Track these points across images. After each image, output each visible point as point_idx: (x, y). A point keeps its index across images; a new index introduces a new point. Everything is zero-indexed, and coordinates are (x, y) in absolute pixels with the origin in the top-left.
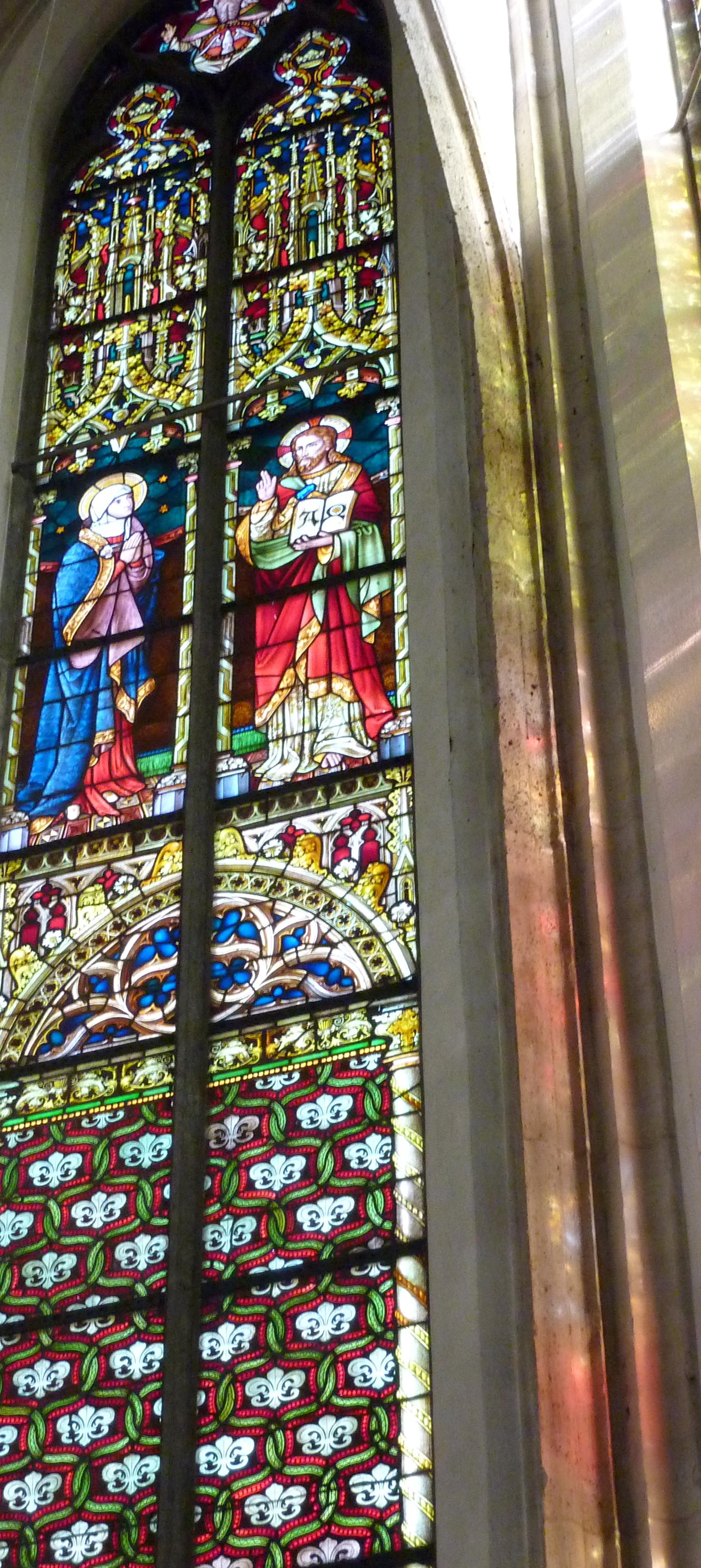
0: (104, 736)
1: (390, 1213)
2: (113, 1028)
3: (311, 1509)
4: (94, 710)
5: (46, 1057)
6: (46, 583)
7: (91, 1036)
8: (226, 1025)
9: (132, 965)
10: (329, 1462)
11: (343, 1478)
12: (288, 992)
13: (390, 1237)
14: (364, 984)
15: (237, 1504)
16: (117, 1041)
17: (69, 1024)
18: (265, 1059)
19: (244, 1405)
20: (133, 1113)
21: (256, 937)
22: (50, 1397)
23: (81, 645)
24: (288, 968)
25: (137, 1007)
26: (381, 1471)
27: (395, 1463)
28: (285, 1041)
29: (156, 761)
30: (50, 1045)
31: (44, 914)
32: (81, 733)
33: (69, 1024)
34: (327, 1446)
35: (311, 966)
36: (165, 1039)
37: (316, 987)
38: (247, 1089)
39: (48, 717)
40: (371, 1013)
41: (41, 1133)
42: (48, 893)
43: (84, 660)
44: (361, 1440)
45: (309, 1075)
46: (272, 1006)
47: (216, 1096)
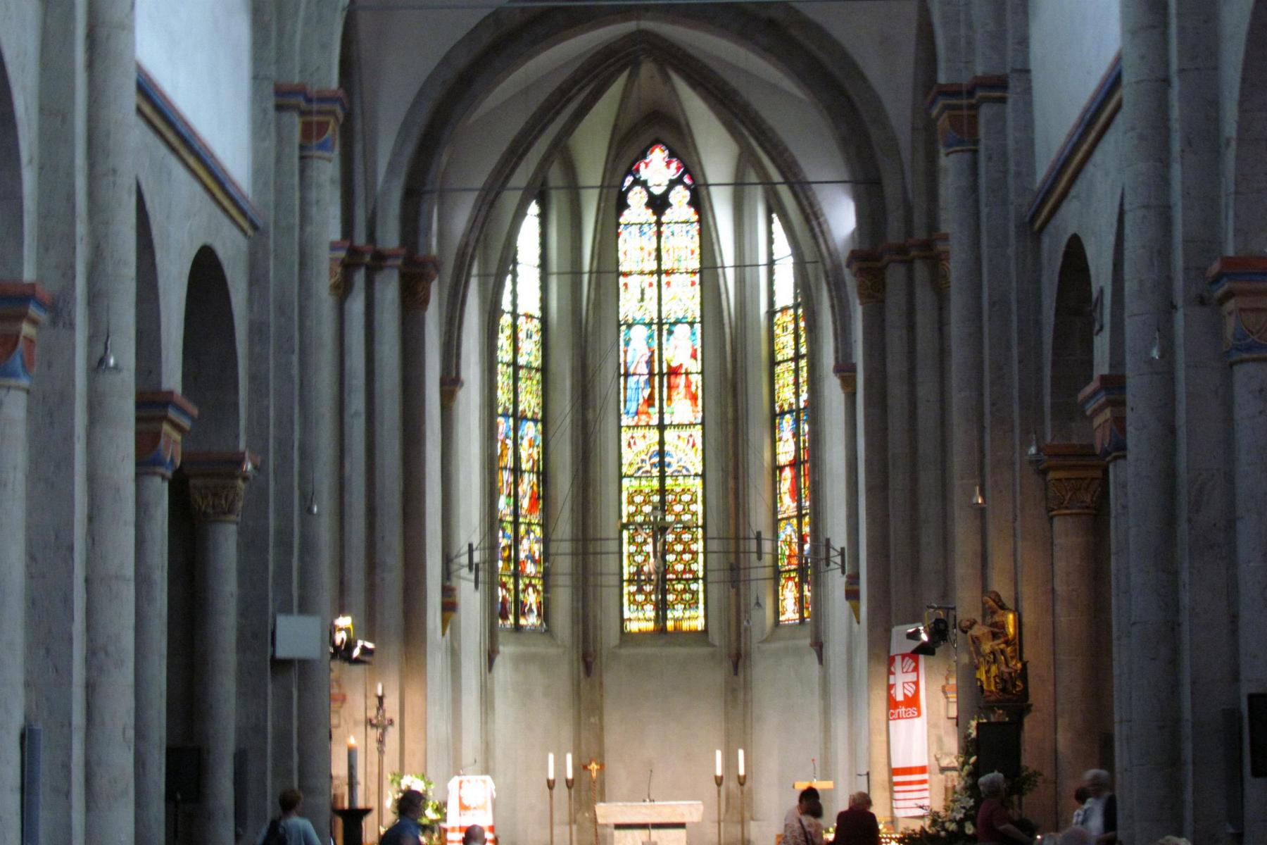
0: (641, 401)
1: (697, 519)
2: (647, 472)
3: (685, 568)
4: (638, 394)
5: (635, 475)
6: (626, 352)
7: (643, 472)
8: (668, 476)
9: (650, 458)
10: (688, 561)
11: (690, 565)
12: (679, 471)
13: (697, 524)
14: (693, 473)
15: (673, 566)
16: (649, 475)
17: (639, 469)
18: (676, 485)
19: (673, 550)
20: (652, 491)
21: (672, 457)
22: (641, 543)
23: (634, 374)
24: (680, 466)
25: (652, 468)
26: (696, 564)
27: (698, 563)
28: (678, 482)
29: (651, 410)
30: (636, 472)
31: (632, 443)
32: (636, 399)
33: (639, 469)
34: (687, 560)
35: (684, 467)
36: (657, 476)
37: (685, 472)
38: (672, 490)
39: (629, 392)
40: (694, 479)
41: (636, 491)
42: (632, 437)
43: (636, 378)
44: (692, 559)
45: (683, 490)
46: (676, 474)
47: (667, 490)
